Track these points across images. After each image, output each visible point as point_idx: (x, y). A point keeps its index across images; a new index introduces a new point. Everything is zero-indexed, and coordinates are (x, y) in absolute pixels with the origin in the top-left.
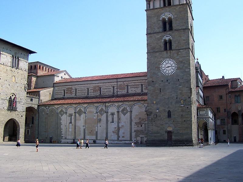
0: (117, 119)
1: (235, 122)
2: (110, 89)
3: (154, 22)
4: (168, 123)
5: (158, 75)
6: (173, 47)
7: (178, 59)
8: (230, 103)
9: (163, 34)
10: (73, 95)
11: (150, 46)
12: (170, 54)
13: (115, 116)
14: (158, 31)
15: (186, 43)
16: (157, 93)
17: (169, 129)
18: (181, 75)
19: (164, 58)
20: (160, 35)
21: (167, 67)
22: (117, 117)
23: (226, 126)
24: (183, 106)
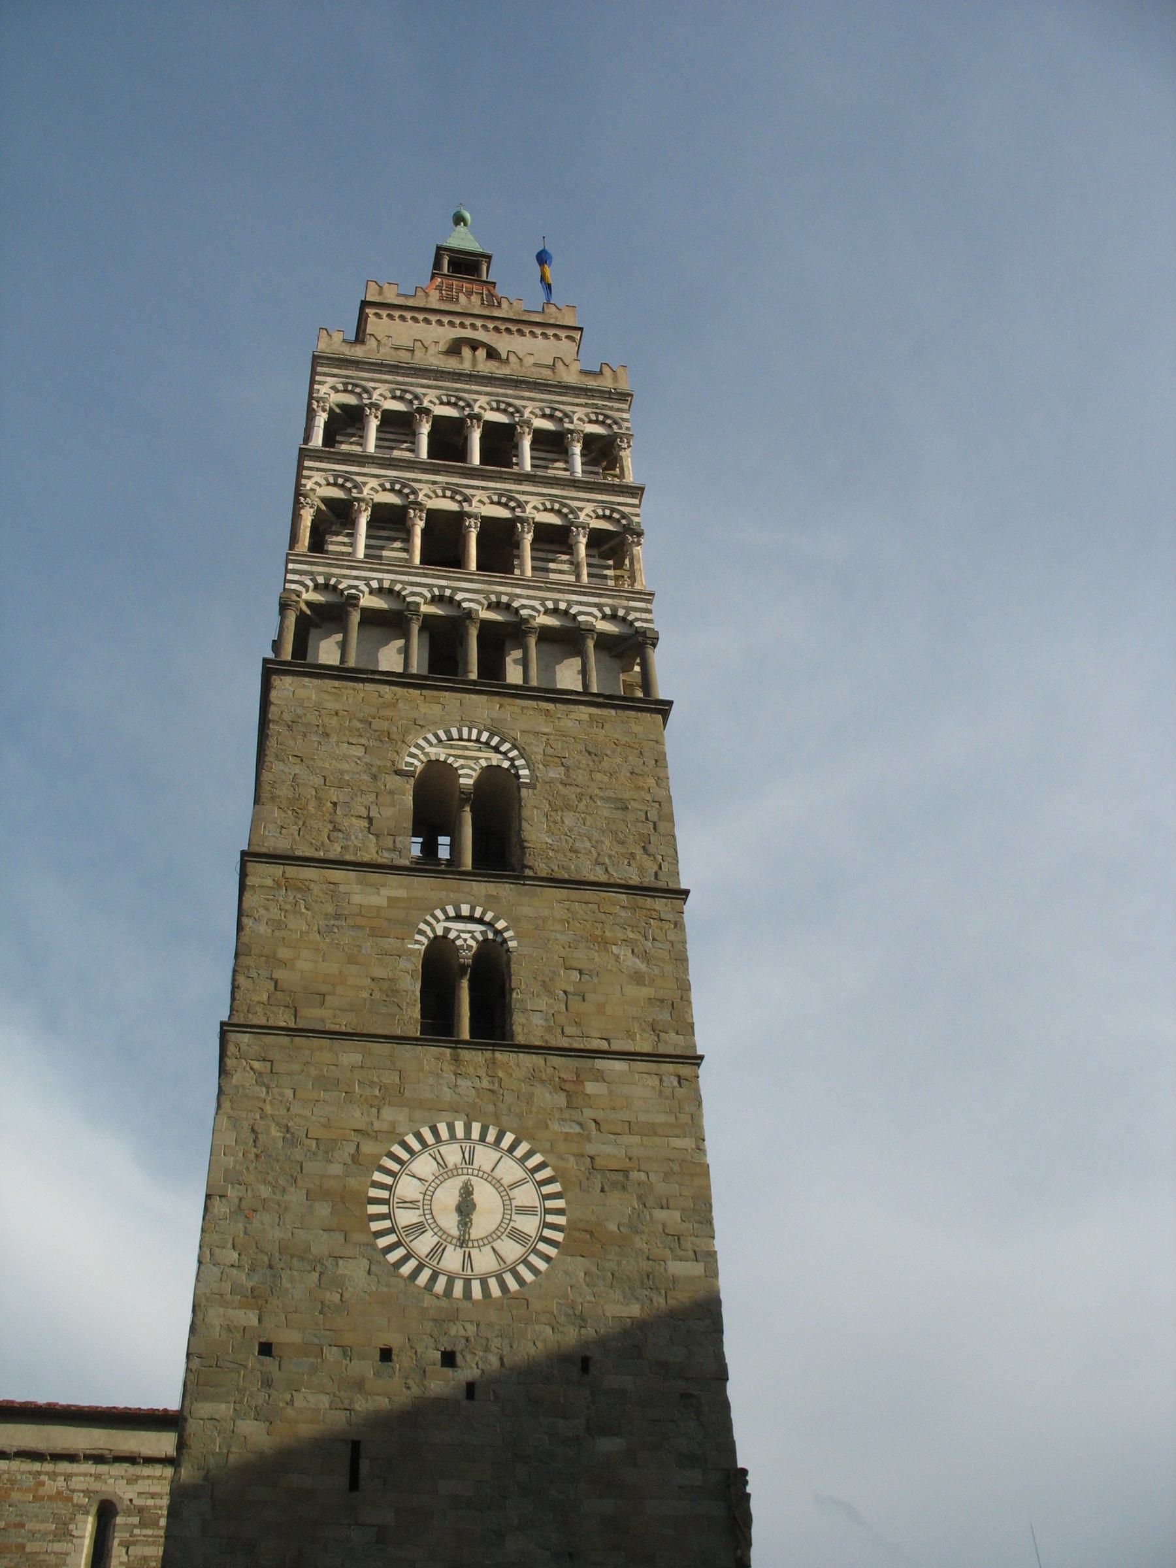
5: (339, 1283)
19: (432, 1108)
20: (395, 888)
21: (467, 1192)
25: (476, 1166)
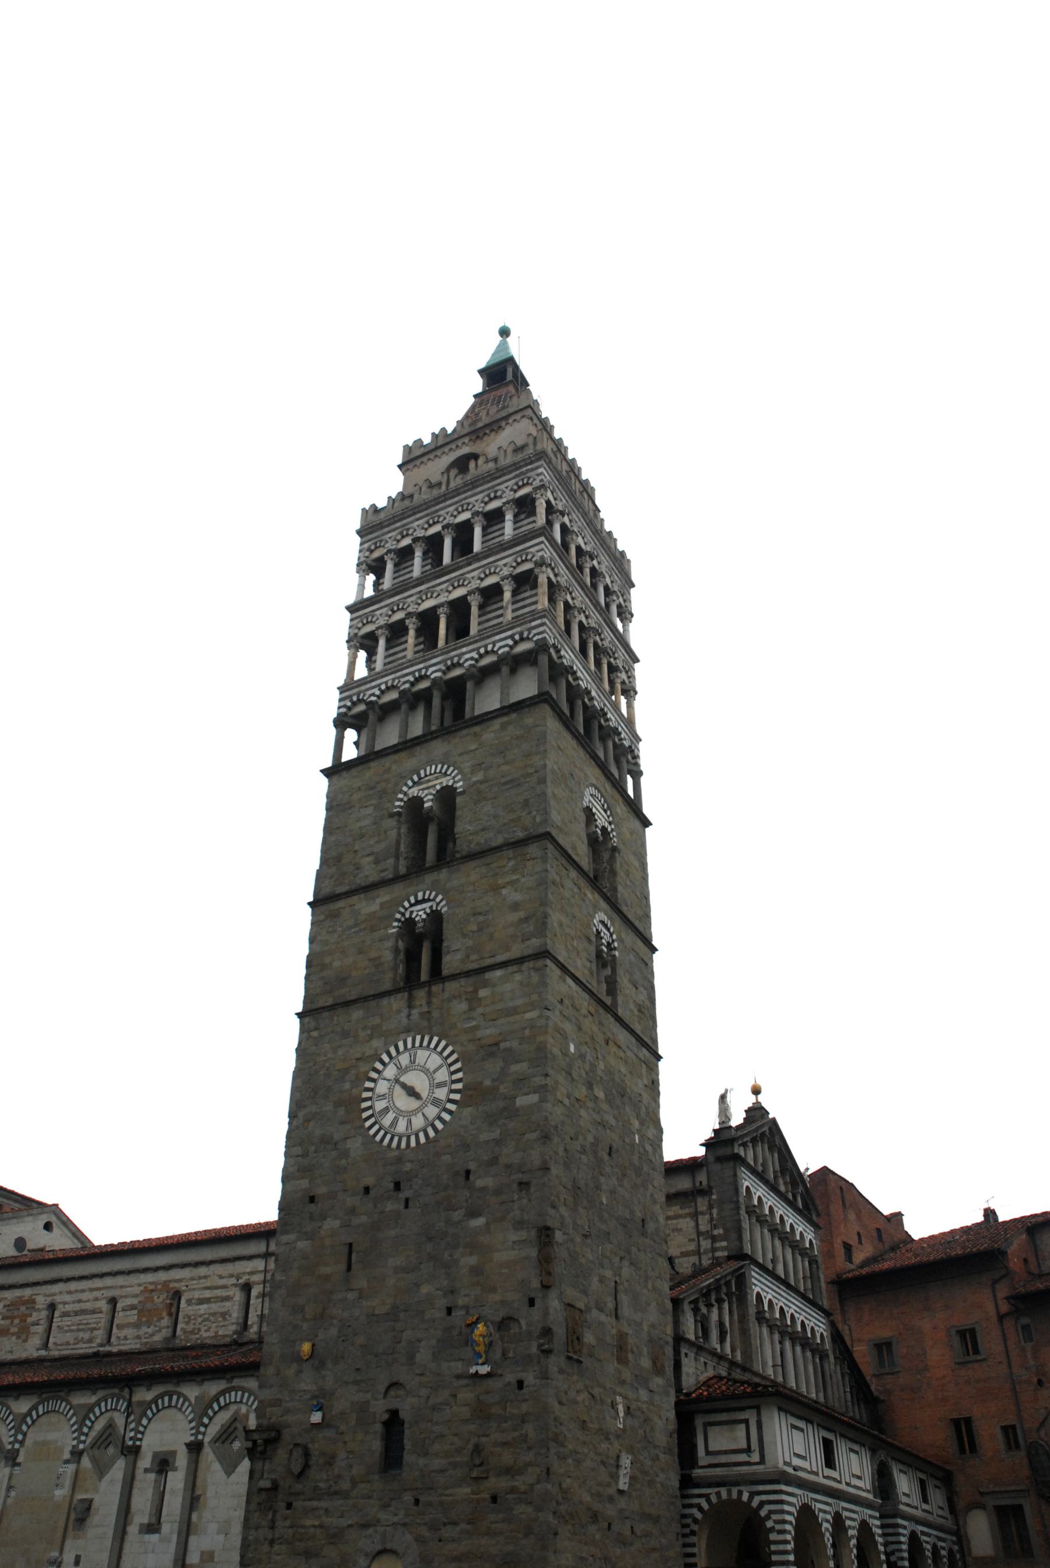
0: (180, 1499)
2: (227, 1299)
3: (361, 828)
5: (346, 1154)
6: (451, 962)
7: (476, 1028)
8: (1035, 1380)
10: (31, 1349)
11: (324, 967)
12: (429, 1003)
13: (176, 1480)
14: (374, 877)
15: (526, 919)
16: (327, 1278)
18: (484, 1137)
22: (181, 1486)
24: (484, 1369)
25: (417, 1063)
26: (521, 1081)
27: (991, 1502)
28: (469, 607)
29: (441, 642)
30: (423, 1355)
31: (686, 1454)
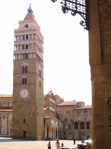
1: (76, 128)
4: (24, 126)
5: (18, 98)
6: (27, 82)
9: (22, 75)
16: (18, 108)
17: (25, 130)
18: (31, 99)
19: (23, 88)
23: (71, 130)
26: (34, 95)
27: (68, 125)
28: (25, 36)
29: (25, 49)
30: (27, 115)
31: (44, 122)
